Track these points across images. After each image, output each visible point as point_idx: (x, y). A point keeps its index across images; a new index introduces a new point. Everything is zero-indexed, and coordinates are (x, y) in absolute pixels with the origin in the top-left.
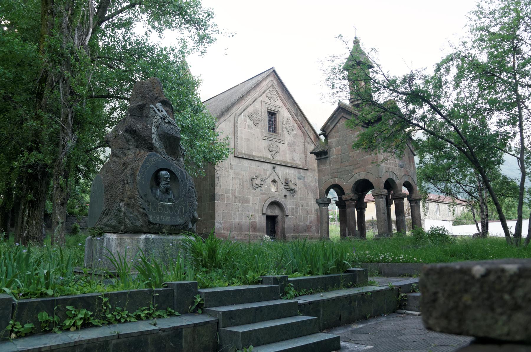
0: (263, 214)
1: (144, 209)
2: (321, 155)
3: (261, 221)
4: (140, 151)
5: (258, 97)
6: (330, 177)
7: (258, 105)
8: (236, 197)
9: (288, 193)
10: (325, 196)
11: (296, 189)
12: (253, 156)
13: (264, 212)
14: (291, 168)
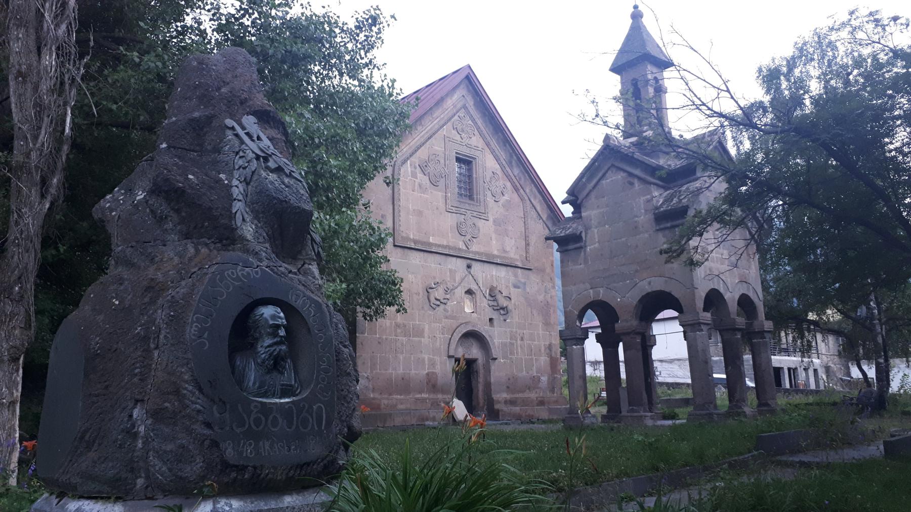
0: (450, 357)
1: (208, 425)
2: (569, 243)
3: (445, 370)
4: (197, 251)
5: (438, 130)
6: (588, 286)
7: (436, 145)
9: (495, 316)
10: (578, 324)
11: (510, 307)
12: (430, 244)
13: (451, 353)
14: (499, 267)
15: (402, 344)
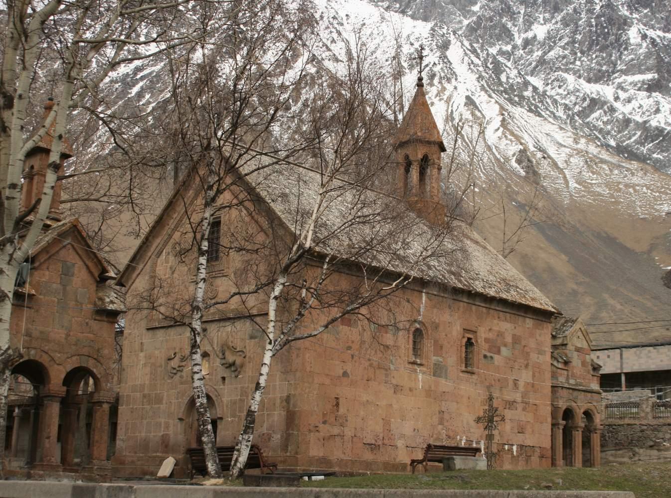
8: (144, 396)
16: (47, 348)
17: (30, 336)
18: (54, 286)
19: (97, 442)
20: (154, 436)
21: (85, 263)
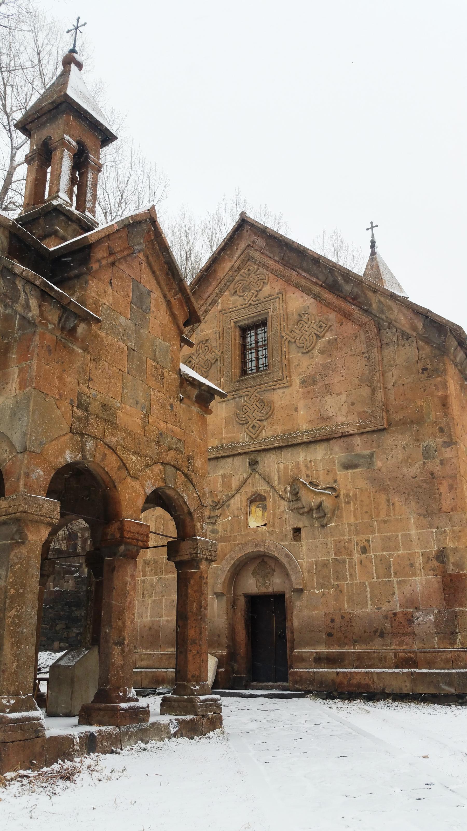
14: (312, 447)
15: (152, 586)
16: (114, 439)
17: (86, 410)
18: (122, 320)
19: (194, 642)
20: (168, 621)
21: (165, 296)
